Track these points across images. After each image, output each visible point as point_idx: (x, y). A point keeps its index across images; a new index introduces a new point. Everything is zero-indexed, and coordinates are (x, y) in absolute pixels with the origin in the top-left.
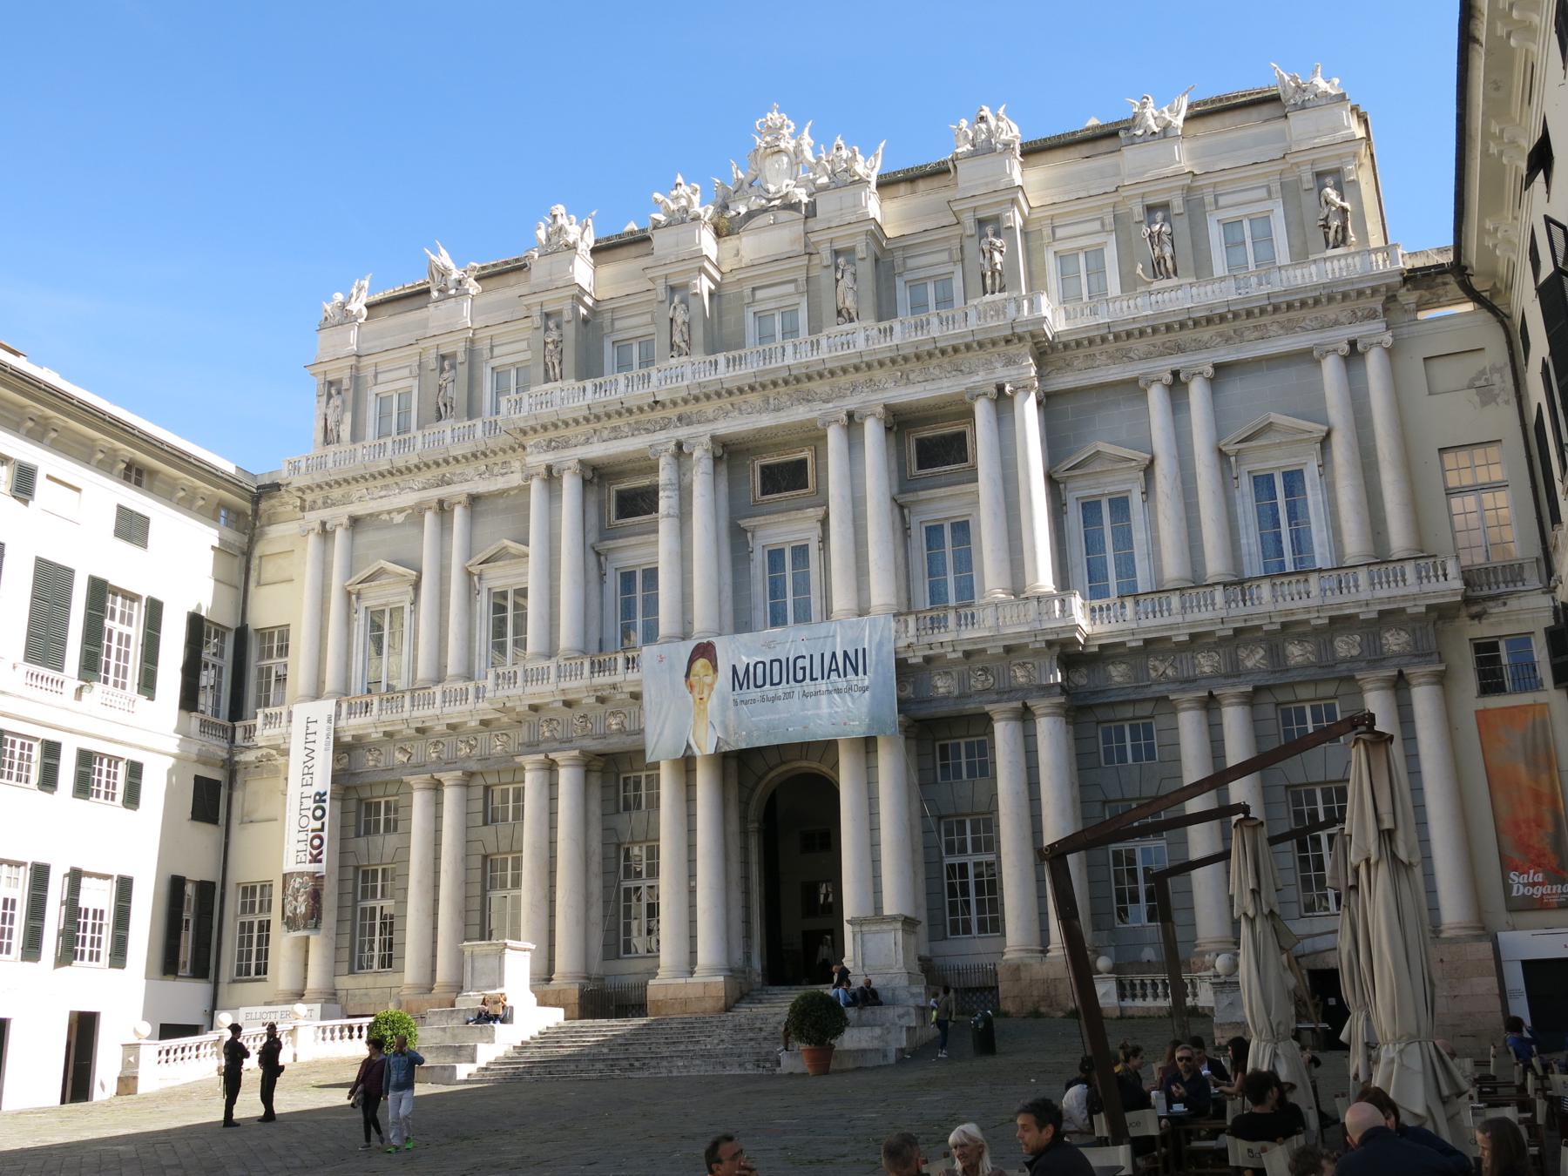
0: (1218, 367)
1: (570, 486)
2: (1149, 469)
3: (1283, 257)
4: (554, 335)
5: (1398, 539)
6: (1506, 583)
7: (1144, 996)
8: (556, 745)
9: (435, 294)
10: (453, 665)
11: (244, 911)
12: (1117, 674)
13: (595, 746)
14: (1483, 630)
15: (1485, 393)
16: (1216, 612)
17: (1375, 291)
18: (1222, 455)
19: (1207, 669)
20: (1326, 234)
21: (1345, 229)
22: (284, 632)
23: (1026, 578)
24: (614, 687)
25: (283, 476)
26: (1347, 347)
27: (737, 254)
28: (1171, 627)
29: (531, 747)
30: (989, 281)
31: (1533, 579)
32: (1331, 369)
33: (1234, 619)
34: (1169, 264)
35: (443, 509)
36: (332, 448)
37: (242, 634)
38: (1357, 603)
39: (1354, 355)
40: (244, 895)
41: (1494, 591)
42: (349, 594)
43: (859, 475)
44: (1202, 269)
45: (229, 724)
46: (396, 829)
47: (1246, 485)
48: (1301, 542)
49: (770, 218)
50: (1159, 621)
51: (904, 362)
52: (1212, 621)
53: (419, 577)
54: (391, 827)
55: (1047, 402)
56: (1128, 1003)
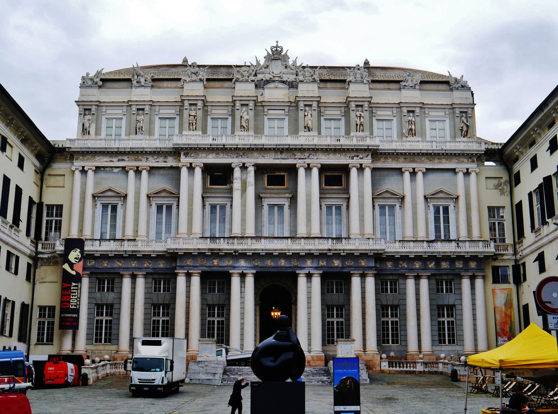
0: (426, 169)
1: (198, 172)
2: (403, 198)
3: (448, 139)
4: (193, 113)
5: (476, 234)
6: (503, 250)
7: (396, 367)
8: (191, 268)
9: (134, 82)
10: (142, 231)
12: (389, 265)
14: (497, 264)
15: (502, 193)
16: (422, 249)
17: (476, 154)
18: (426, 198)
19: (417, 267)
20: (462, 132)
21: (467, 131)
22: (60, 208)
23: (362, 229)
24: (219, 250)
25: (68, 145)
26: (466, 171)
27: (262, 95)
28: (409, 252)
29: (182, 267)
30: (358, 127)
31: (511, 251)
33: (428, 252)
34: (413, 132)
35: (138, 172)
36: (86, 137)
37: (40, 205)
38: (465, 252)
39: (467, 173)
40: (40, 310)
41: (500, 252)
42: (94, 197)
43: (308, 185)
44: (423, 134)
45: (35, 241)
46: (112, 291)
47: (432, 210)
48: (447, 229)
49: (276, 84)
50: (406, 250)
51: (328, 150)
52: (422, 252)
53: (126, 195)
54: (111, 289)
55: (374, 170)
56: (391, 369)
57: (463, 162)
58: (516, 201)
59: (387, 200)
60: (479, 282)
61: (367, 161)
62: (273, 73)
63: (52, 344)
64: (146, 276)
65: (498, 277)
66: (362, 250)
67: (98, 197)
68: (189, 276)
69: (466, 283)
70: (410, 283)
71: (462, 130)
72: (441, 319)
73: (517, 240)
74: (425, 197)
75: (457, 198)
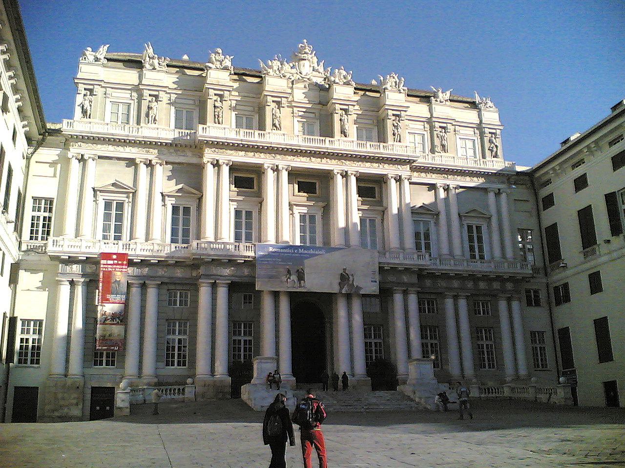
1: (225, 170)
2: (438, 214)
9: (147, 66)
11: (22, 333)
12: (428, 283)
13: (237, 280)
17: (508, 175)
20: (491, 152)
29: (208, 276)
32: (491, 196)
38: (505, 273)
39: (498, 194)
47: (466, 228)
48: (481, 249)
55: (410, 183)
57: (494, 182)
58: (546, 223)
59: (424, 216)
60: (515, 305)
61: (404, 171)
63: (39, 367)
64: (159, 287)
65: (532, 300)
66: (406, 265)
67: (101, 191)
68: (214, 286)
69: (503, 305)
70: (449, 303)
71: (492, 151)
72: (480, 343)
73: (547, 263)
74: (459, 214)
75: (490, 218)
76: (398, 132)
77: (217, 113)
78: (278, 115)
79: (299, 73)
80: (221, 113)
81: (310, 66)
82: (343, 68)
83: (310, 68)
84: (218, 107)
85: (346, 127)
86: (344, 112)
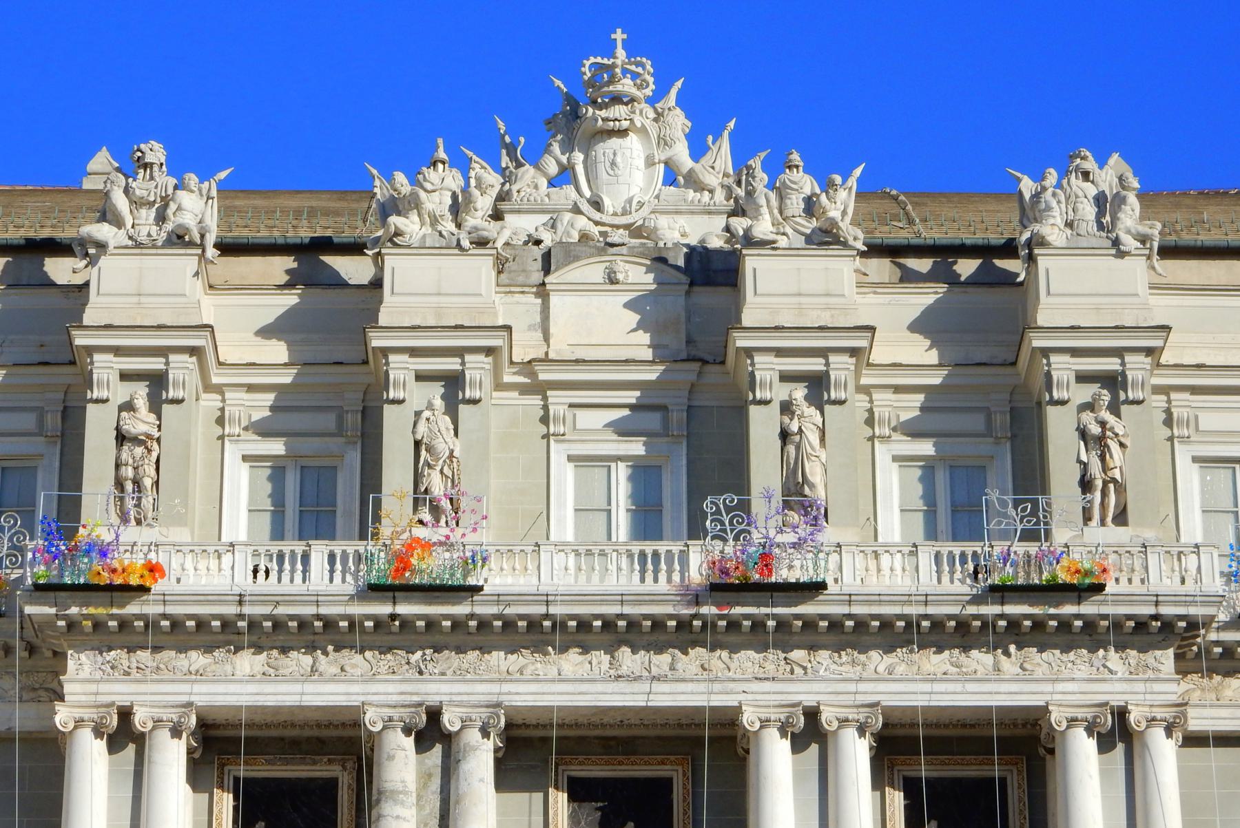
62: (597, 205)
76: (1105, 469)
77: (129, 472)
78: (445, 442)
79: (585, 207)
80: (151, 471)
81: (650, 162)
82: (796, 157)
83: (649, 170)
84: (136, 440)
85: (814, 472)
86: (799, 392)
